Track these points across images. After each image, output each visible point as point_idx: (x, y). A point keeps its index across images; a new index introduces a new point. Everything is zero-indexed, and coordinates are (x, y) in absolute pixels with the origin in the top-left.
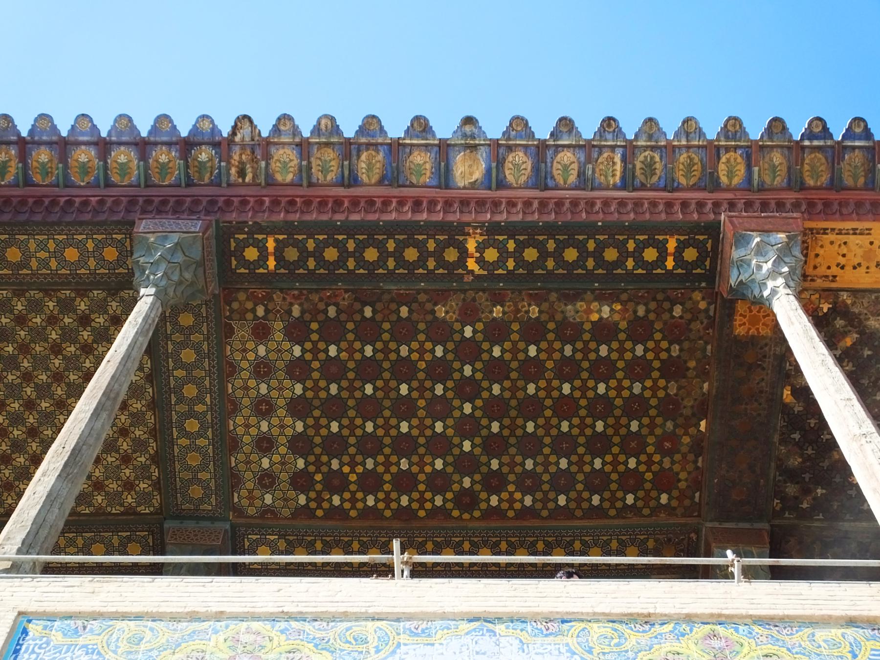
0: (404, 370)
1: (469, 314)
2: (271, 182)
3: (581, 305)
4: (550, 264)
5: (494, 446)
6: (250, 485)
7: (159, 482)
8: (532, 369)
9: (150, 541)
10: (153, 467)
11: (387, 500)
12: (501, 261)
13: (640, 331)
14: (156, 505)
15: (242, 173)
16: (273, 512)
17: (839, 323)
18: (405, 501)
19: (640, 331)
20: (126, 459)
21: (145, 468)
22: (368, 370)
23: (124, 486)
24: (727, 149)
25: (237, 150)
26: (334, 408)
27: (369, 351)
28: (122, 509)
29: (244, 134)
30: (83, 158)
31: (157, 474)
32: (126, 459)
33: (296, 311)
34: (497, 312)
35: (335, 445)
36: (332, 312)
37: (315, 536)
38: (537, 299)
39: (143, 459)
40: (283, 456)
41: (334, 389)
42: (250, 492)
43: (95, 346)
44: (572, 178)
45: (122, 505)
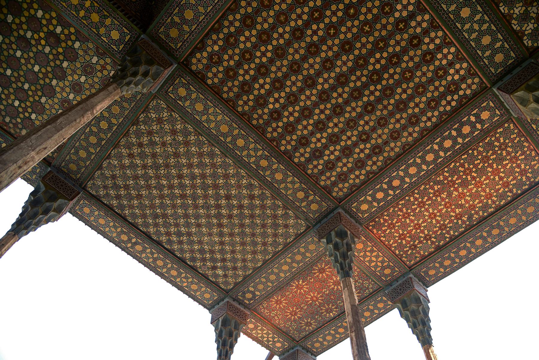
6: (99, 74)
7: (144, 110)
9: (171, 89)
10: (141, 120)
14: (155, 102)
16: (97, 51)
20: (150, 133)
21: (145, 123)
23: (162, 122)
28: (173, 113)
31: (142, 115)
32: (150, 133)
37: (81, 20)
39: (142, 127)
40: (72, 75)
42: (101, 71)
43: (122, 186)
45: (171, 115)
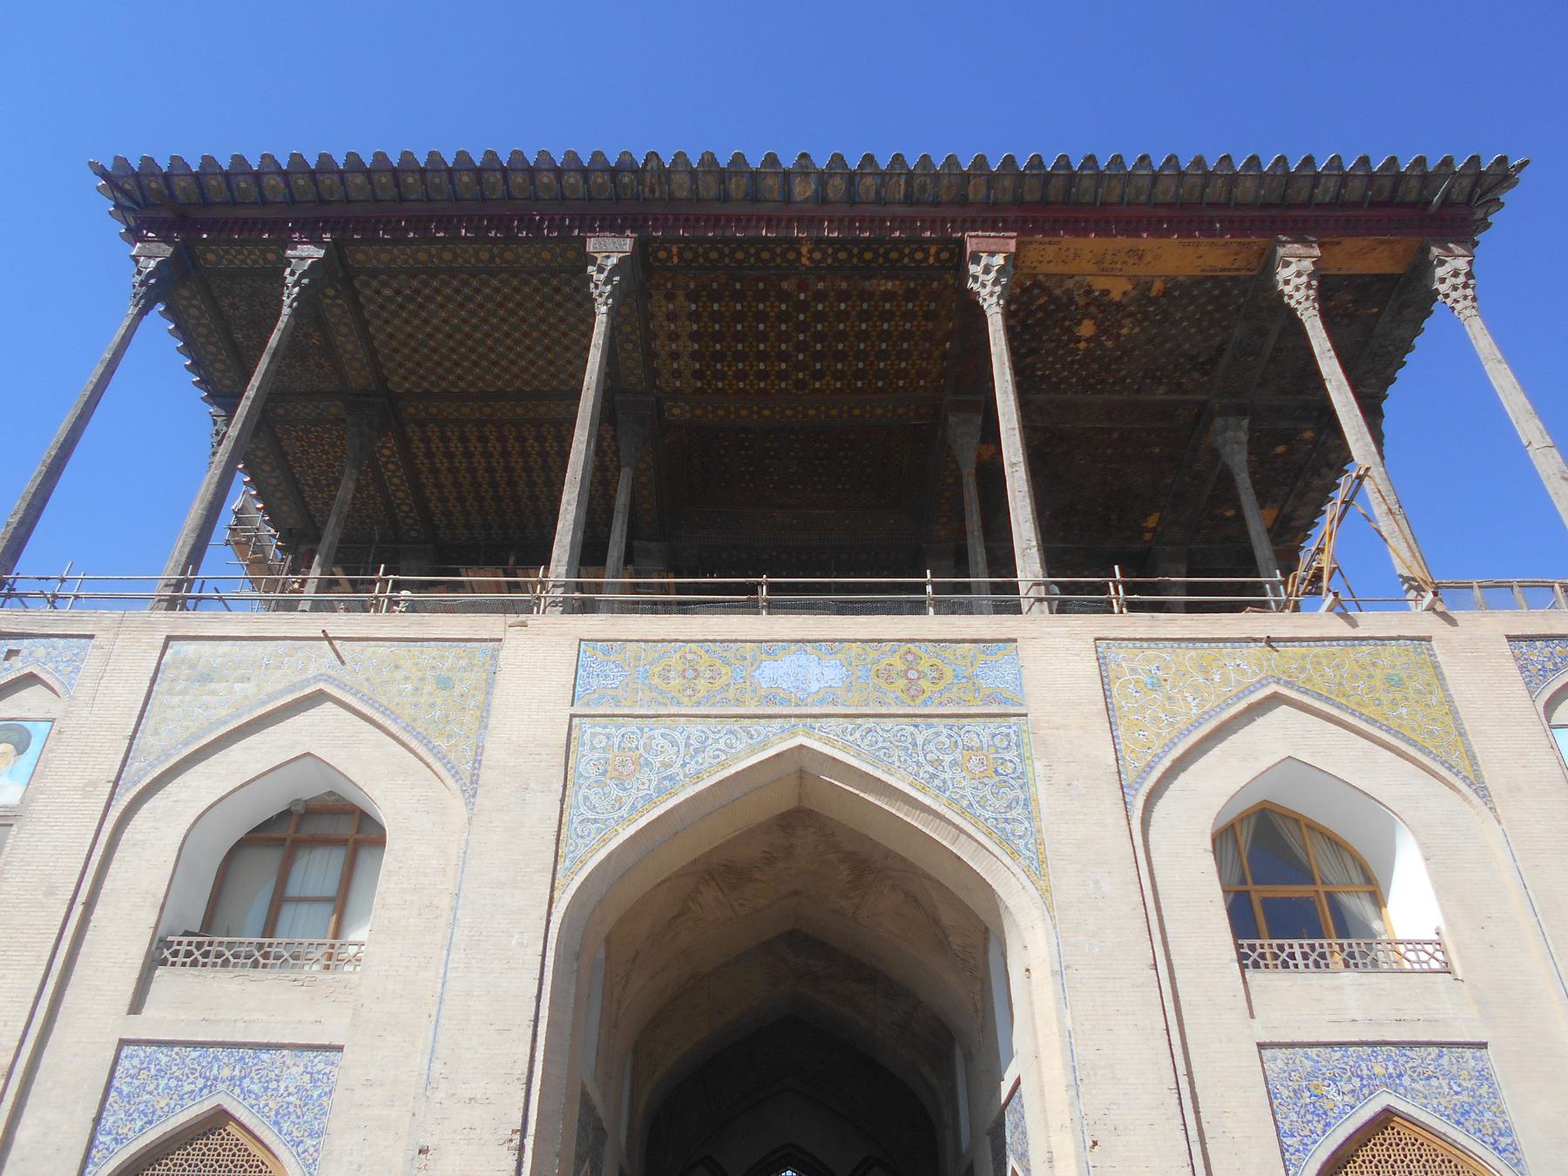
0: (761, 317)
1: (802, 286)
2: (672, 198)
3: (874, 282)
4: (855, 261)
5: (817, 357)
8: (842, 316)
11: (752, 385)
12: (824, 259)
13: (910, 295)
15: (652, 191)
17: (1036, 292)
18: (762, 385)
19: (910, 295)
22: (738, 317)
24: (976, 176)
25: (648, 175)
26: (718, 337)
27: (739, 307)
29: (653, 164)
30: (545, 180)
33: (692, 285)
34: (821, 286)
35: (719, 357)
36: (715, 286)
38: (845, 278)
41: (717, 327)
44: (872, 194)
